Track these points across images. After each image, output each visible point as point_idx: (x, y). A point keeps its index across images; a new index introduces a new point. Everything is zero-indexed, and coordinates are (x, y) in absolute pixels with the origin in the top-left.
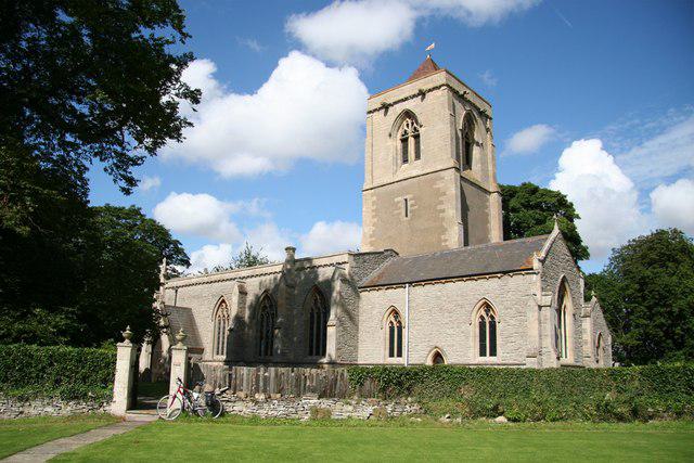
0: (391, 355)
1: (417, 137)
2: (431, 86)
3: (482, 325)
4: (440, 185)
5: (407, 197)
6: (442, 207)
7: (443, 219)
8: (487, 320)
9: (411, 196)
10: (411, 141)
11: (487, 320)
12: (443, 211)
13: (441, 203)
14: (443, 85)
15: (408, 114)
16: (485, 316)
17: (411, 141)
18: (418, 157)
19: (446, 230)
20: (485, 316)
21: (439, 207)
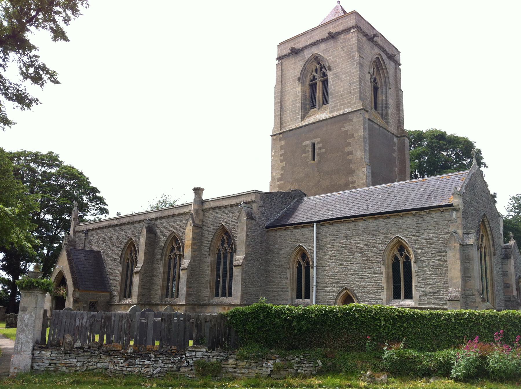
0: (397, 296)
1: (325, 82)
2: (340, 28)
3: (395, 266)
4: (348, 127)
5: (315, 140)
6: (349, 149)
7: (351, 161)
8: (401, 260)
9: (319, 139)
10: (319, 86)
11: (401, 260)
12: (351, 153)
13: (349, 144)
14: (353, 27)
15: (316, 59)
16: (398, 256)
17: (319, 86)
18: (325, 101)
19: (354, 171)
20: (398, 256)
21: (347, 149)
